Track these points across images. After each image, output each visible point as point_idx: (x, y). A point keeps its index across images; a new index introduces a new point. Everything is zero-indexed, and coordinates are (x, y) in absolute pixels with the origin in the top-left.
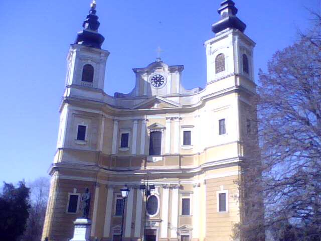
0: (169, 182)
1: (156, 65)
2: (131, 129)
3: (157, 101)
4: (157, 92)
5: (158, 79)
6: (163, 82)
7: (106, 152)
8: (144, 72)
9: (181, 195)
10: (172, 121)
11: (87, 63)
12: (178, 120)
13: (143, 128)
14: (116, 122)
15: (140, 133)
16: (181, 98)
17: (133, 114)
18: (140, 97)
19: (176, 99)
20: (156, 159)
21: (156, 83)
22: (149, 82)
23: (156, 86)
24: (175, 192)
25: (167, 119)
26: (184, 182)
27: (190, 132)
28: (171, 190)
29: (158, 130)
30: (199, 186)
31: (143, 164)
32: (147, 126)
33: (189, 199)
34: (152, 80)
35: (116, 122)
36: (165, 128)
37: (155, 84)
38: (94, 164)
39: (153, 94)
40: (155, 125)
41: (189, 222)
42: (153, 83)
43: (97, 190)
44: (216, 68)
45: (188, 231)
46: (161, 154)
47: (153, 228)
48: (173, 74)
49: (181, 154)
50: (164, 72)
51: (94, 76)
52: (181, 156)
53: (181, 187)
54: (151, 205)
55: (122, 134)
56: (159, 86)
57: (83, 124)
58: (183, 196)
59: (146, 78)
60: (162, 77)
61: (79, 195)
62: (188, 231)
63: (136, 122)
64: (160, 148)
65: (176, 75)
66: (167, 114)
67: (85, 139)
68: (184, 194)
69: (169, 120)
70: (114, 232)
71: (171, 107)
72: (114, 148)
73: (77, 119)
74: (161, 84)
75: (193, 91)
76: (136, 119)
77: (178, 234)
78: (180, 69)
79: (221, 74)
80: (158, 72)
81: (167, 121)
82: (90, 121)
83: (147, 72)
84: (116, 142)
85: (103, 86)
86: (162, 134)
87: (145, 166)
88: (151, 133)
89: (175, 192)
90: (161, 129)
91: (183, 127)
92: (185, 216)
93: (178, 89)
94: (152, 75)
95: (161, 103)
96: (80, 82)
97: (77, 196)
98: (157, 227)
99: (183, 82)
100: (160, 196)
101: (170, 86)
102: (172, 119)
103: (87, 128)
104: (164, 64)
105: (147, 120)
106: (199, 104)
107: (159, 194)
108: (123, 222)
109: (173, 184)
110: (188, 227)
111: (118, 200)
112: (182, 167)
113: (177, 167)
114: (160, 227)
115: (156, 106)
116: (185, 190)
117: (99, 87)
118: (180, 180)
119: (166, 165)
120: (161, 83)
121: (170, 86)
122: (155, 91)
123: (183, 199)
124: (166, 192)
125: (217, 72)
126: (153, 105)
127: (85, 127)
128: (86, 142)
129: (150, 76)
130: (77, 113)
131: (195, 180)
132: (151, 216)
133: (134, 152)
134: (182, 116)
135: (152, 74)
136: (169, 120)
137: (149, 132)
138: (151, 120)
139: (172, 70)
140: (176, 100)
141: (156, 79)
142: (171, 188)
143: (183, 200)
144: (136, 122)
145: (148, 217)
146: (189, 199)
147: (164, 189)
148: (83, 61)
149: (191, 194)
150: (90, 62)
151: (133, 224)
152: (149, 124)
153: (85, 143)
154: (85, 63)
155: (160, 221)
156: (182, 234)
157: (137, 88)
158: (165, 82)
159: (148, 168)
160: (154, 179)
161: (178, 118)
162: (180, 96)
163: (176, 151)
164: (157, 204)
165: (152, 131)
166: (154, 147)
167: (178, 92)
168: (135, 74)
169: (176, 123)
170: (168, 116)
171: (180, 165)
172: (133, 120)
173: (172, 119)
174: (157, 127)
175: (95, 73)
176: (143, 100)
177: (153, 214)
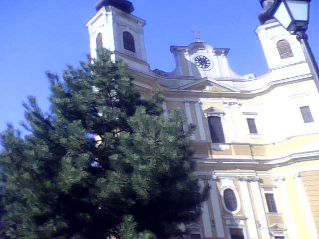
0: (247, 174)
1: (196, 46)
3: (208, 83)
8: (185, 52)
9: (262, 189)
10: (230, 106)
12: (237, 105)
13: (197, 109)
16: (234, 82)
17: (182, 95)
18: (187, 77)
19: (230, 84)
20: (223, 147)
21: (201, 64)
22: (193, 61)
23: (202, 67)
24: (254, 185)
25: (225, 103)
26: (261, 175)
27: (253, 119)
28: (249, 183)
29: (216, 115)
30: (284, 180)
31: (209, 153)
32: (203, 110)
33: (272, 194)
34: (196, 60)
37: (201, 66)
39: (203, 76)
40: (211, 109)
41: (279, 220)
45: (281, 231)
46: (226, 142)
47: (240, 227)
48: (219, 57)
49: (251, 143)
50: (208, 52)
52: (251, 146)
53: (260, 181)
54: (229, 200)
56: (206, 68)
58: (265, 190)
59: (190, 58)
60: (206, 58)
62: (281, 231)
63: (187, 104)
64: (223, 135)
65: (224, 59)
66: (223, 98)
68: (266, 188)
69: (227, 105)
71: (224, 91)
75: (246, 77)
76: (187, 101)
77: (271, 235)
78: (227, 52)
80: (201, 53)
81: (224, 105)
83: (188, 51)
86: (223, 121)
87: (211, 154)
88: (208, 117)
89: (254, 185)
90: (219, 114)
92: (273, 214)
93: (228, 73)
94: (195, 55)
95: (214, 86)
98: (242, 226)
99: (233, 66)
100: (236, 189)
101: (218, 69)
102: (230, 104)
104: (209, 46)
105: (201, 103)
106: (263, 90)
107: (236, 187)
109: (250, 177)
110: (280, 225)
112: (256, 158)
113: (249, 157)
115: (208, 89)
116: (265, 184)
118: (257, 172)
121: (218, 69)
122: (203, 73)
124: (243, 185)
126: (204, 88)
129: (192, 56)
131: (275, 173)
132: (233, 213)
134: (240, 101)
135: (195, 54)
136: (227, 105)
137: (206, 117)
138: (207, 103)
139: (218, 52)
140: (230, 84)
141: (200, 59)
142: (248, 181)
143: (267, 195)
144: (187, 104)
145: (232, 215)
146: (272, 194)
147: (240, 182)
149: (273, 189)
151: (213, 221)
152: (205, 107)
155: (245, 219)
156: (276, 235)
158: (212, 64)
159: (215, 157)
160: (225, 170)
161: (236, 103)
162: (233, 80)
164: (234, 198)
165: (209, 115)
166: (216, 134)
171: (252, 156)
172: (184, 102)
173: (230, 104)
174: (214, 112)
177: (233, 210)
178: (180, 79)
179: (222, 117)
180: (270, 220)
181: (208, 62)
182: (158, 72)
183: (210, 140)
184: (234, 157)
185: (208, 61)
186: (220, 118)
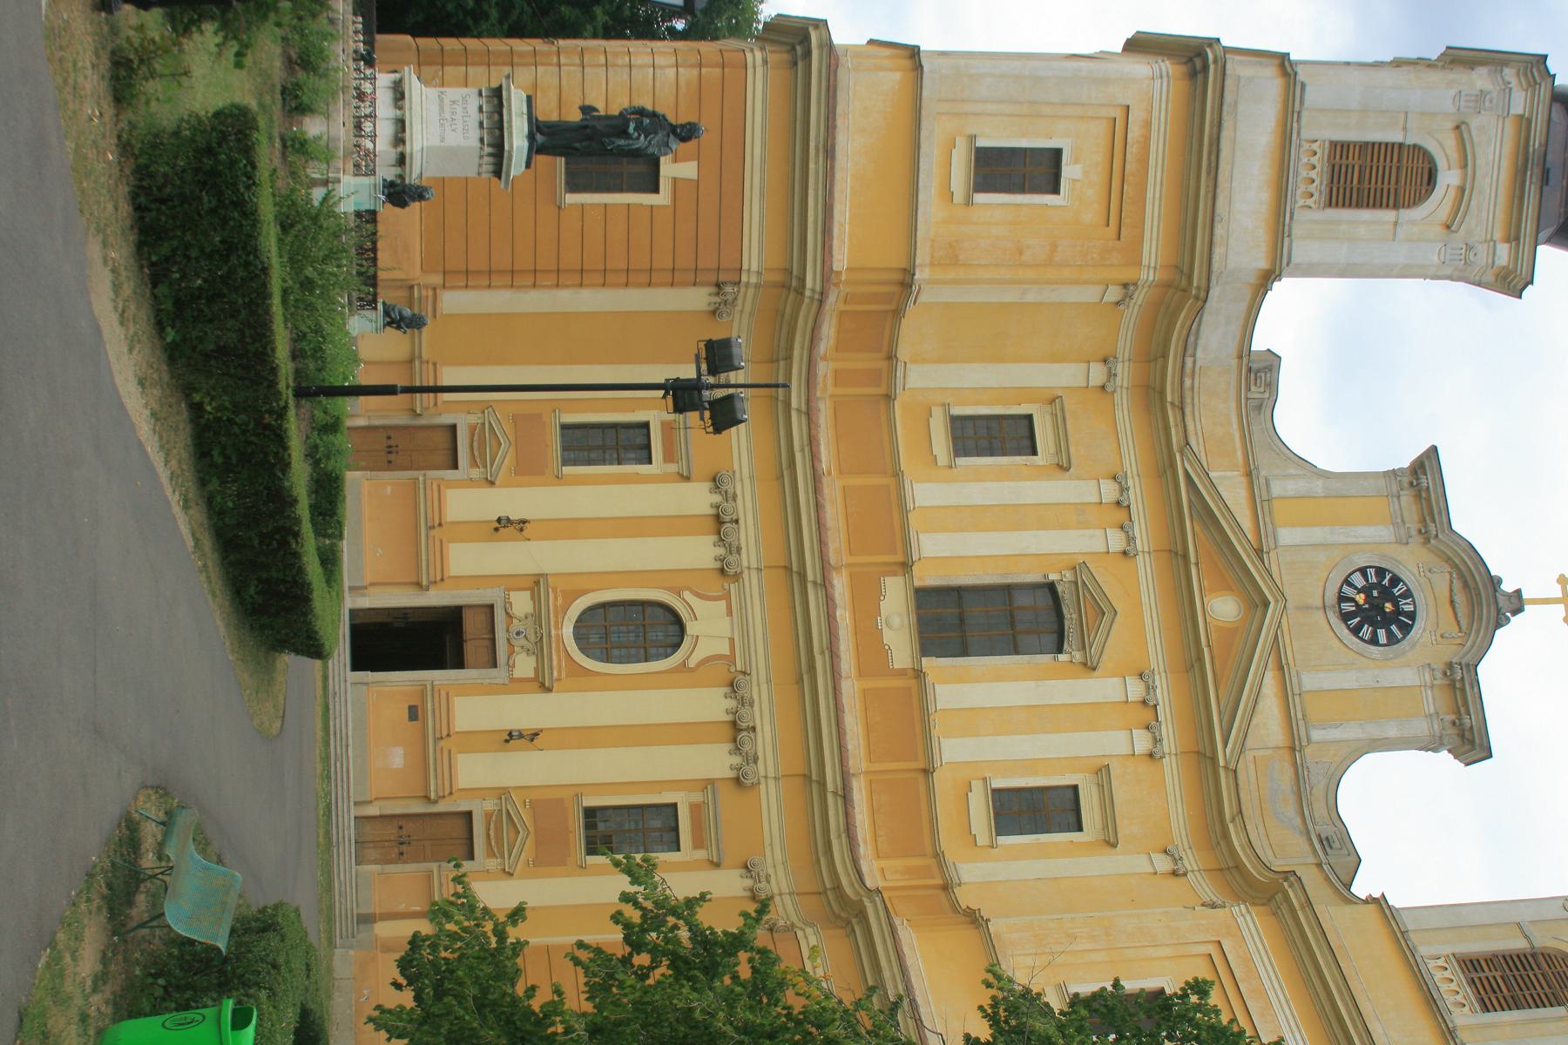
2: (1063, 467)
4: (1307, 608)
5: (1388, 607)
6: (1374, 641)
7: (913, 332)
11: (1441, 163)
14: (1097, 374)
15: (1042, 526)
24: (717, 761)
35: (1097, 374)
36: (1089, 667)
38: (841, 260)
42: (1358, 580)
43: (697, 299)
44: (1492, 960)
46: (933, 665)
51: (1365, 214)
55: (1029, 418)
56: (1345, 617)
57: (1070, 171)
60: (1406, 629)
61: (662, 198)
67: (981, 198)
69: (1136, 690)
70: (473, 429)
72: (943, 377)
73: (1099, 130)
74: (1356, 631)
79: (1453, 989)
82: (1091, 215)
84: (985, 385)
85: (1310, 271)
86: (1046, 659)
91: (1102, 773)
96: (1319, 130)
97: (656, 190)
98: (511, 666)
103: (1049, 199)
107: (692, 663)
108: (529, 470)
111: (646, 425)
114: (516, 685)
117: (1301, 250)
119: (865, 692)
120: (1366, 631)
123: (675, 805)
125: (1471, 965)
127: (1056, 190)
128: (969, 202)
130: (1135, 132)
133: (925, 493)
134: (1171, 768)
141: (1386, 593)
148: (1451, 142)
150: (1448, 178)
153: (959, 197)
154: (1443, 150)
157: (1318, 486)
163: (953, 750)
167: (1316, 735)
168: (1405, 461)
169: (1114, 741)
170: (1160, 682)
175: (1388, 215)
176: (1247, 524)
178: (1249, 474)
179: (1062, 657)
180: (546, 805)
181: (1382, 633)
182: (1260, 373)
183: (927, 577)
184: (850, 689)
185: (1392, 640)
186: (1060, 650)
